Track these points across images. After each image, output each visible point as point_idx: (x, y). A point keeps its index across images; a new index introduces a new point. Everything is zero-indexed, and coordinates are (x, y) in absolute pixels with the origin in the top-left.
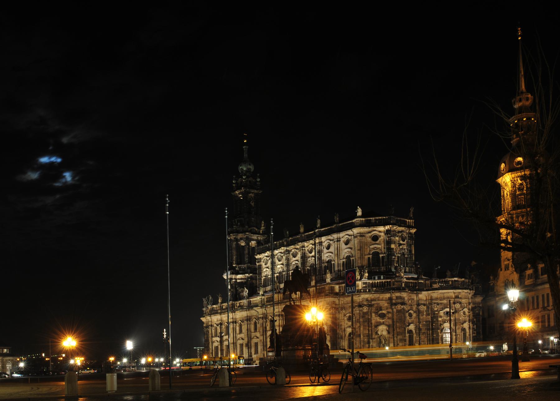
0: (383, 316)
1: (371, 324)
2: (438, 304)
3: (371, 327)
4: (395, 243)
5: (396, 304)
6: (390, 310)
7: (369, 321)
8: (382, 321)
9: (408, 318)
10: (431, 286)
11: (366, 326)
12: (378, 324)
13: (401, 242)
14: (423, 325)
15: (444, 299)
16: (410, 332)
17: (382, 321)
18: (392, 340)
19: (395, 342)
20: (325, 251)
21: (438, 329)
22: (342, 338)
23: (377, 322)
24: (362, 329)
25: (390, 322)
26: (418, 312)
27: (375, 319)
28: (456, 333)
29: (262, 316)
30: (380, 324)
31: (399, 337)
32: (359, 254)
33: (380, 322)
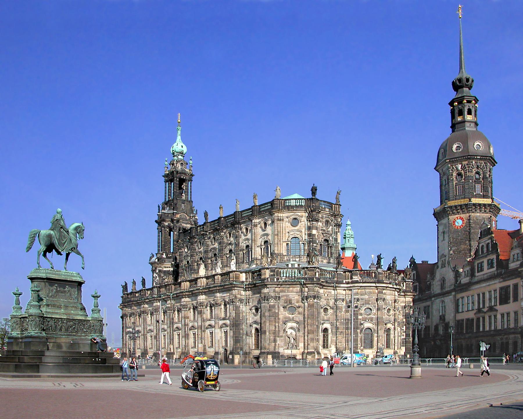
1: (279, 319)
2: (358, 300)
4: (317, 229)
6: (301, 304)
10: (352, 278)
11: (271, 321)
14: (341, 322)
16: (325, 330)
19: (306, 341)
22: (247, 334)
23: (285, 318)
25: (301, 318)
26: (336, 308)
27: (283, 314)
28: (377, 334)
31: (310, 336)
32: (276, 240)
33: (289, 317)
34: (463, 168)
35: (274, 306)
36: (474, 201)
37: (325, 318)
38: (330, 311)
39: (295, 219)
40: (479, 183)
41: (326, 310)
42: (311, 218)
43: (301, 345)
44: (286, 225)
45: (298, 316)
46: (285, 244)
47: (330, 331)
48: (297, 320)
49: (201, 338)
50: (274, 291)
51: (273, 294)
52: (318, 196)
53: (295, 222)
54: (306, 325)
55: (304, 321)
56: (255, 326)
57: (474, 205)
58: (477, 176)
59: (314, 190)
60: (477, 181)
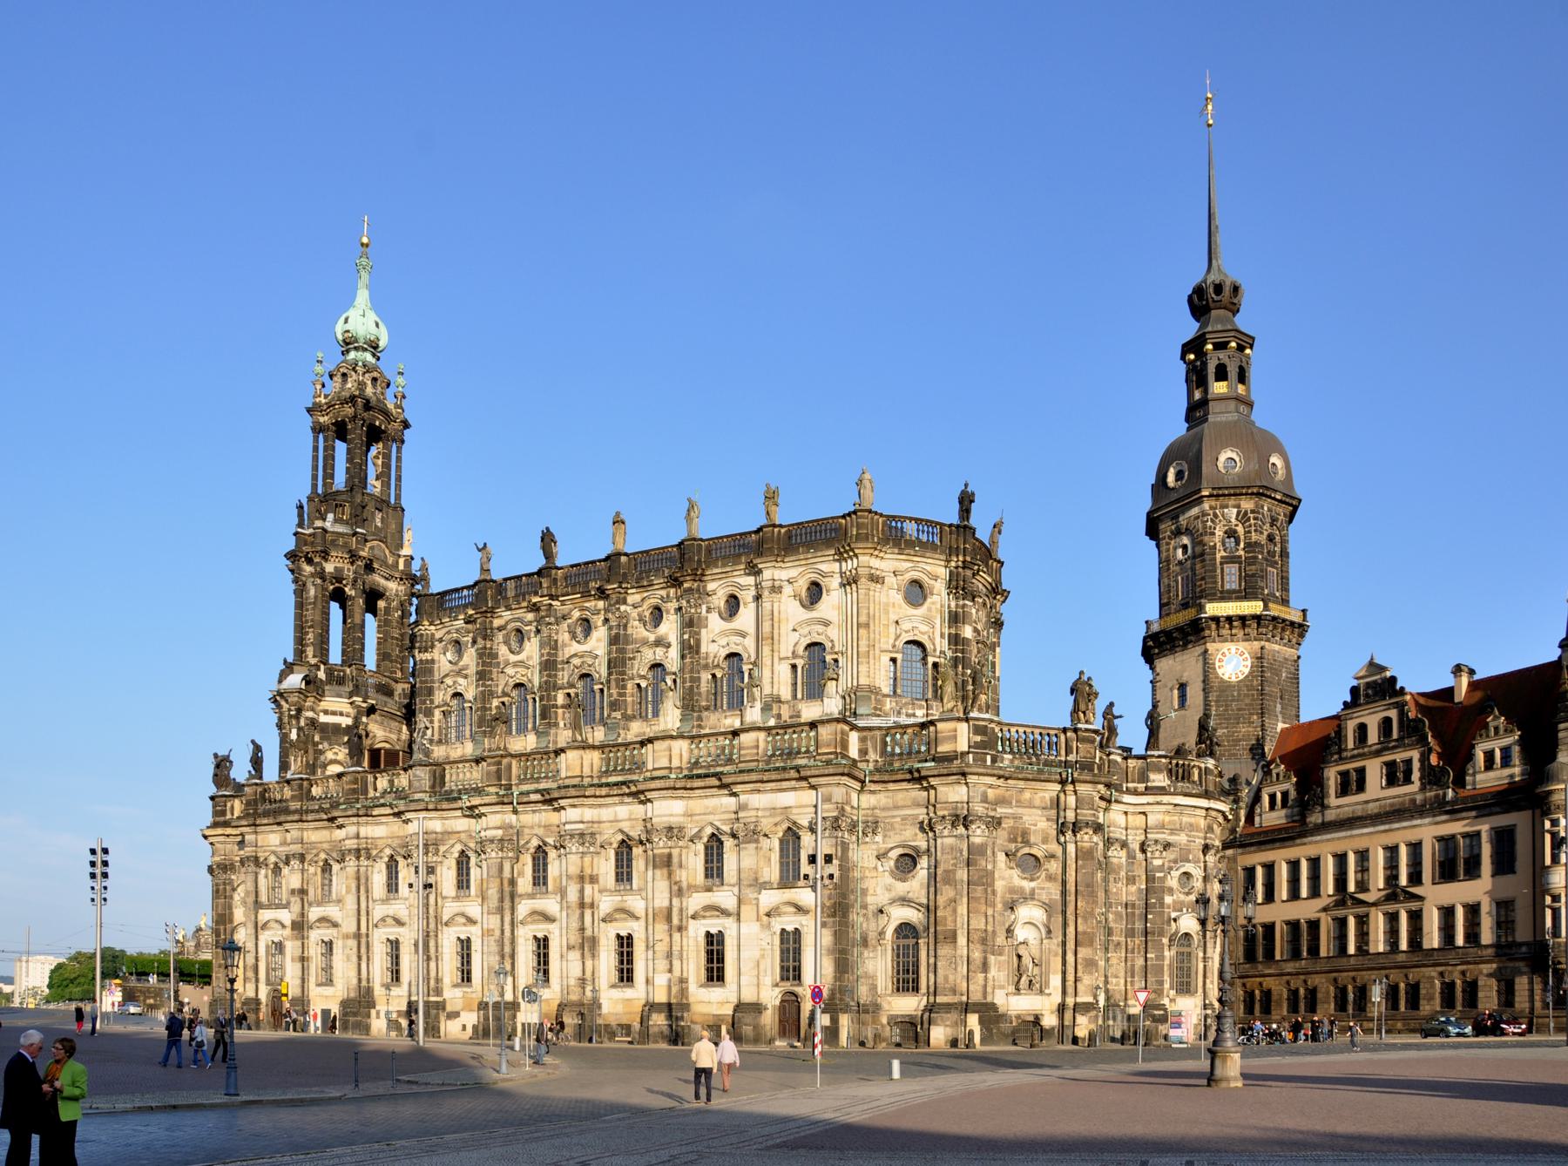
1: (994, 892)
2: (1167, 846)
3: (994, 906)
7: (987, 879)
8: (1028, 885)
11: (977, 899)
14: (1117, 914)
15: (1181, 829)
17: (1028, 885)
21: (1161, 934)
22: (865, 942)
23: (1012, 890)
24: (962, 909)
25: (1054, 891)
27: (1007, 876)
29: (500, 833)
34: (1243, 517)
40: (1273, 565)
43: (1055, 981)
45: (1048, 884)
48: (1044, 898)
49: (669, 955)
54: (1071, 918)
55: (1065, 903)
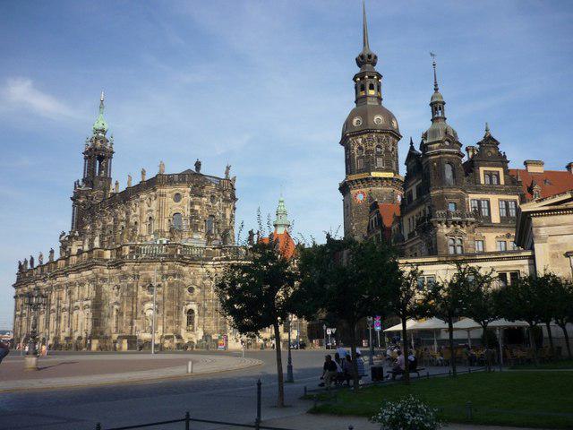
0: (150, 288)
4: (200, 204)
5: (167, 276)
7: (133, 296)
8: (150, 296)
9: (188, 293)
12: (146, 301)
13: (210, 204)
16: (191, 312)
17: (150, 296)
18: (161, 322)
20: (133, 213)
22: (109, 317)
24: (125, 305)
25: (160, 298)
27: (142, 293)
30: (148, 300)
31: (170, 318)
34: (364, 141)
35: (131, 286)
36: (374, 174)
37: (191, 298)
38: (197, 291)
39: (178, 194)
41: (191, 290)
42: (194, 193)
43: (160, 328)
44: (169, 199)
46: (166, 220)
47: (196, 313)
50: (133, 269)
51: (131, 273)
52: (202, 172)
53: (177, 197)
56: (116, 307)
57: (374, 178)
58: (379, 150)
59: (198, 165)
60: (379, 155)
